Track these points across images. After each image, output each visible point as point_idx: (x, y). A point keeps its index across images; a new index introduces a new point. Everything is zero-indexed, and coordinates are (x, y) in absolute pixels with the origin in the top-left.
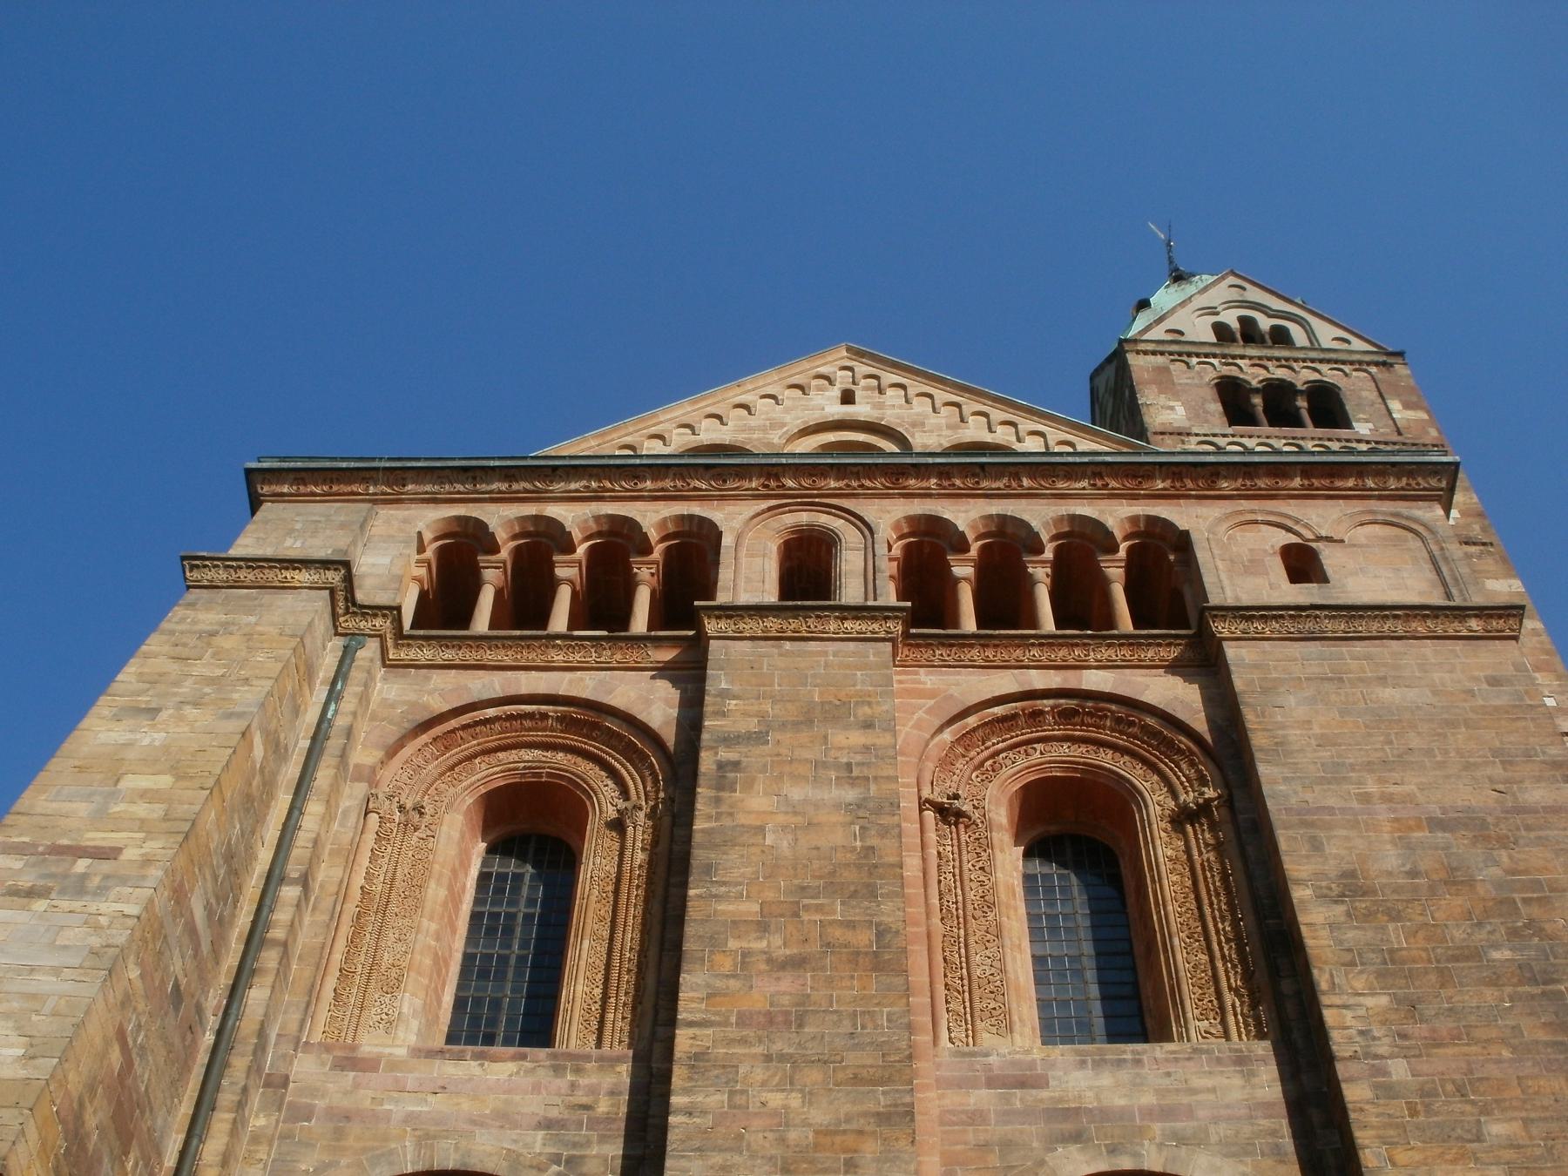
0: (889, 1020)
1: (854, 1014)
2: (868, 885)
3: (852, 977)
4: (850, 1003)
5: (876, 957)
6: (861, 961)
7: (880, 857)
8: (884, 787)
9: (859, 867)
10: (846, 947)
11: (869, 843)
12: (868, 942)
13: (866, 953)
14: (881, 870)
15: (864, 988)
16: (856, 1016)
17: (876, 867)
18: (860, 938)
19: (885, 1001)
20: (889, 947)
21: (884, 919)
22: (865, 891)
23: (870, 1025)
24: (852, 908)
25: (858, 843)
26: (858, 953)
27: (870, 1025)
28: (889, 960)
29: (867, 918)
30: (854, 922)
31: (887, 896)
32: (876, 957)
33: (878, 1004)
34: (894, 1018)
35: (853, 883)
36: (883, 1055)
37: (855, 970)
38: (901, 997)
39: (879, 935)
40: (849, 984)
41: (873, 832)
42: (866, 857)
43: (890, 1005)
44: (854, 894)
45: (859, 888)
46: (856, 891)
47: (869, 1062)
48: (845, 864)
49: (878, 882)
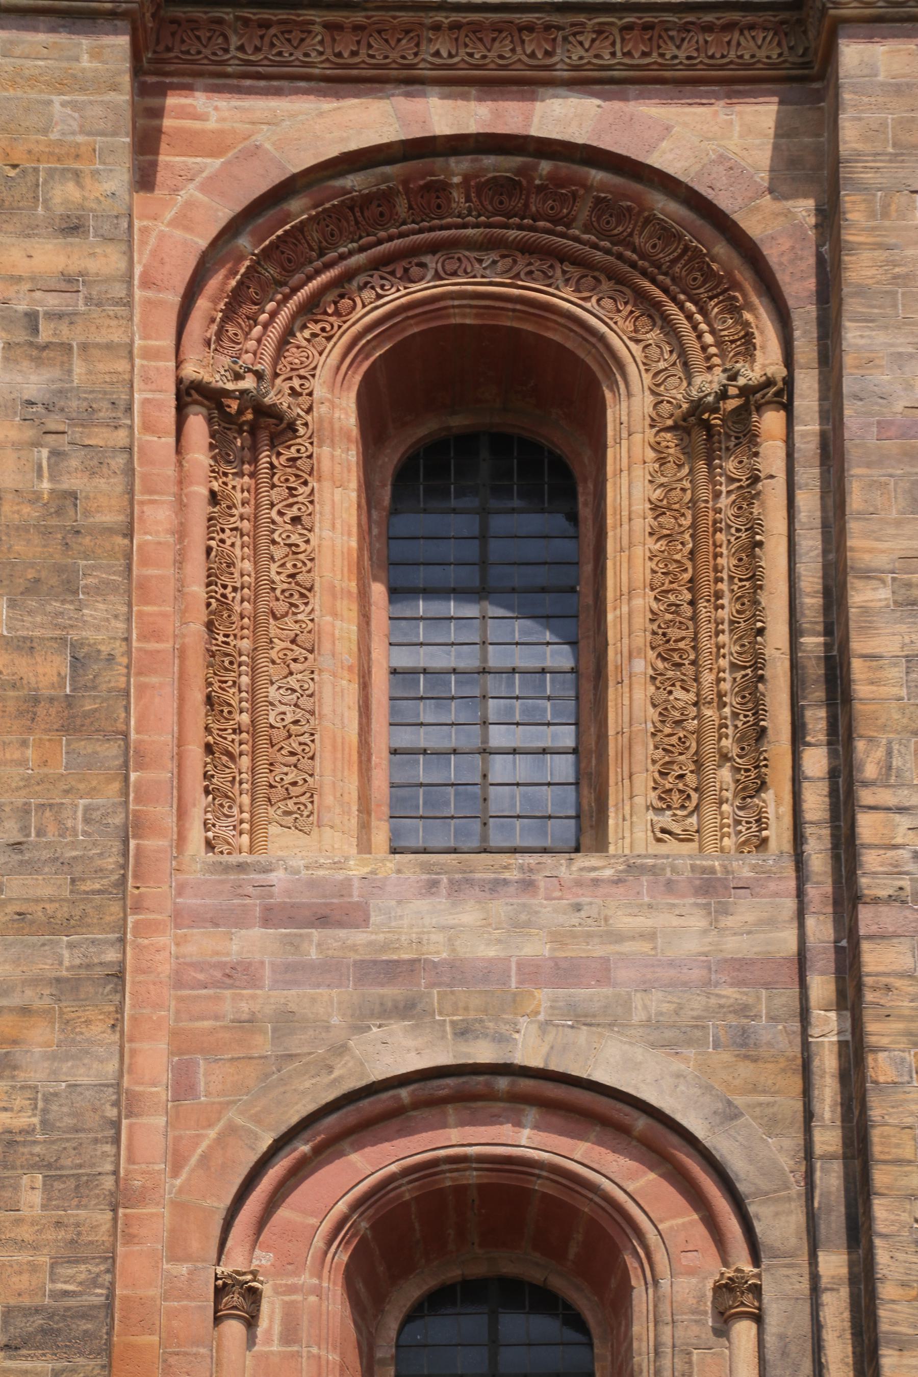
0: (87, 821)
1: (25, 810)
2: (60, 569)
3: (24, 743)
4: (18, 789)
5: (70, 706)
6: (41, 711)
7: (87, 513)
8: (101, 367)
9: (46, 533)
10: (14, 686)
11: (65, 486)
12: (55, 679)
13: (52, 700)
14: (87, 540)
15: (45, 763)
16: (28, 812)
17: (78, 532)
18: (40, 670)
19: (81, 786)
20: (94, 688)
21: (89, 635)
22: (54, 581)
23: (52, 829)
24: (30, 613)
25: (46, 485)
26: (36, 700)
27: (52, 829)
28: (95, 710)
29: (58, 633)
30: (31, 639)
31: (98, 591)
32: (70, 706)
33: (67, 792)
34: (96, 815)
35: (32, 565)
36: (73, 881)
37: (30, 730)
38: (109, 780)
39: (77, 663)
40: (17, 755)
41: (74, 463)
42: (59, 512)
43: (92, 792)
44: (34, 587)
45: (44, 574)
46: (37, 581)
47: (47, 891)
48: (18, 528)
49: (83, 563)
